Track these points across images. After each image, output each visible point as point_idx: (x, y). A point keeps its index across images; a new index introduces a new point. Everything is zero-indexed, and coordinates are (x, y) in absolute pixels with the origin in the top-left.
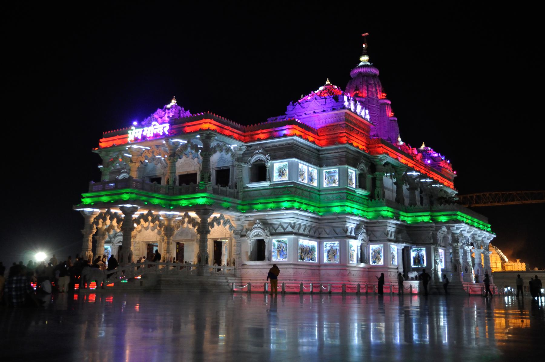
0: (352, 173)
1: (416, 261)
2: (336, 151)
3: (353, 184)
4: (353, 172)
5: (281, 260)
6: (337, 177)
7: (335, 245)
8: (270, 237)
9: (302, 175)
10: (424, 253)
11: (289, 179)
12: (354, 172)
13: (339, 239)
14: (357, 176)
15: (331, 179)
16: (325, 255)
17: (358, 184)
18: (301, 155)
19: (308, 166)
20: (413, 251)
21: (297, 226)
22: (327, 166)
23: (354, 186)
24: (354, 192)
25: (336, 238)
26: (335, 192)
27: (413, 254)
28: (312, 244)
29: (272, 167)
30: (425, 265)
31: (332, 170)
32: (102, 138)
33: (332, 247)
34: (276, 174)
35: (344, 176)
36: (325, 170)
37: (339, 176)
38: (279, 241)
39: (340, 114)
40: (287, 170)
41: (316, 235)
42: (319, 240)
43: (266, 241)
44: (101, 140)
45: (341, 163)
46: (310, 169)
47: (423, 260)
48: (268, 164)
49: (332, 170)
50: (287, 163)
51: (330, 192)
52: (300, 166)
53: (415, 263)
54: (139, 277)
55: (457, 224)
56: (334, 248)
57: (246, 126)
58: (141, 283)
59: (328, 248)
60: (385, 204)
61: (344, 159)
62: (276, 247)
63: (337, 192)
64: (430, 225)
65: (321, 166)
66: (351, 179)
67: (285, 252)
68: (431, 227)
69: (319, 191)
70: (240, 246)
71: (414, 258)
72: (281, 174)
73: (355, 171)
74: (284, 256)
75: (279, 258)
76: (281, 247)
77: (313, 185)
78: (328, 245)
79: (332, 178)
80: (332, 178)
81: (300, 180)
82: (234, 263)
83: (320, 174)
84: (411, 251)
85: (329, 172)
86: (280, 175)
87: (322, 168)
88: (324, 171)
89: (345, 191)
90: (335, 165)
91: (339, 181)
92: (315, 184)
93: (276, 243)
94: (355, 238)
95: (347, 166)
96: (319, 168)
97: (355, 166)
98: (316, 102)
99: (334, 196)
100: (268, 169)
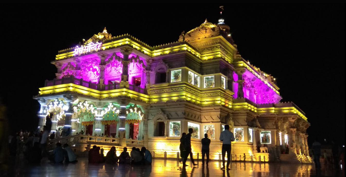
0: (223, 79)
1: (264, 140)
2: (213, 64)
5: (176, 136)
6: (214, 82)
7: (212, 127)
8: (168, 120)
9: (191, 79)
10: (269, 135)
11: (182, 81)
13: (214, 123)
14: (227, 81)
15: (209, 83)
17: (227, 87)
19: (194, 73)
20: (262, 133)
21: (187, 114)
22: (207, 74)
23: (225, 88)
25: (212, 122)
26: (212, 91)
27: (262, 135)
28: (196, 127)
30: (270, 143)
31: (210, 77)
32: (57, 55)
33: (210, 128)
34: (172, 78)
35: (218, 81)
36: (205, 77)
37: (215, 80)
38: (174, 123)
39: (216, 39)
40: (180, 75)
42: (200, 124)
43: (166, 123)
44: (57, 56)
45: (216, 72)
46: (196, 75)
47: (269, 139)
49: (210, 77)
50: (181, 70)
51: (208, 92)
52: (189, 72)
53: (263, 141)
54: (74, 145)
55: (293, 116)
56: (211, 129)
57: (153, 47)
58: (75, 150)
59: (207, 129)
60: (245, 101)
62: (172, 127)
63: (214, 91)
64: (274, 116)
65: (202, 74)
66: (223, 83)
67: (178, 131)
68: (275, 117)
70: (147, 127)
71: (263, 138)
72: (176, 77)
73: (225, 78)
74: (178, 133)
75: (174, 135)
76: (175, 128)
79: (210, 82)
80: (210, 82)
81: (189, 82)
82: (143, 138)
83: (202, 79)
84: (260, 133)
85: (208, 78)
86: (175, 79)
87: (203, 76)
88: (205, 78)
89: (220, 91)
90: (212, 73)
91: (215, 84)
93: (172, 125)
95: (221, 74)
96: (201, 76)
97: (225, 74)
98: (199, 32)
99: (212, 94)
100: (167, 74)
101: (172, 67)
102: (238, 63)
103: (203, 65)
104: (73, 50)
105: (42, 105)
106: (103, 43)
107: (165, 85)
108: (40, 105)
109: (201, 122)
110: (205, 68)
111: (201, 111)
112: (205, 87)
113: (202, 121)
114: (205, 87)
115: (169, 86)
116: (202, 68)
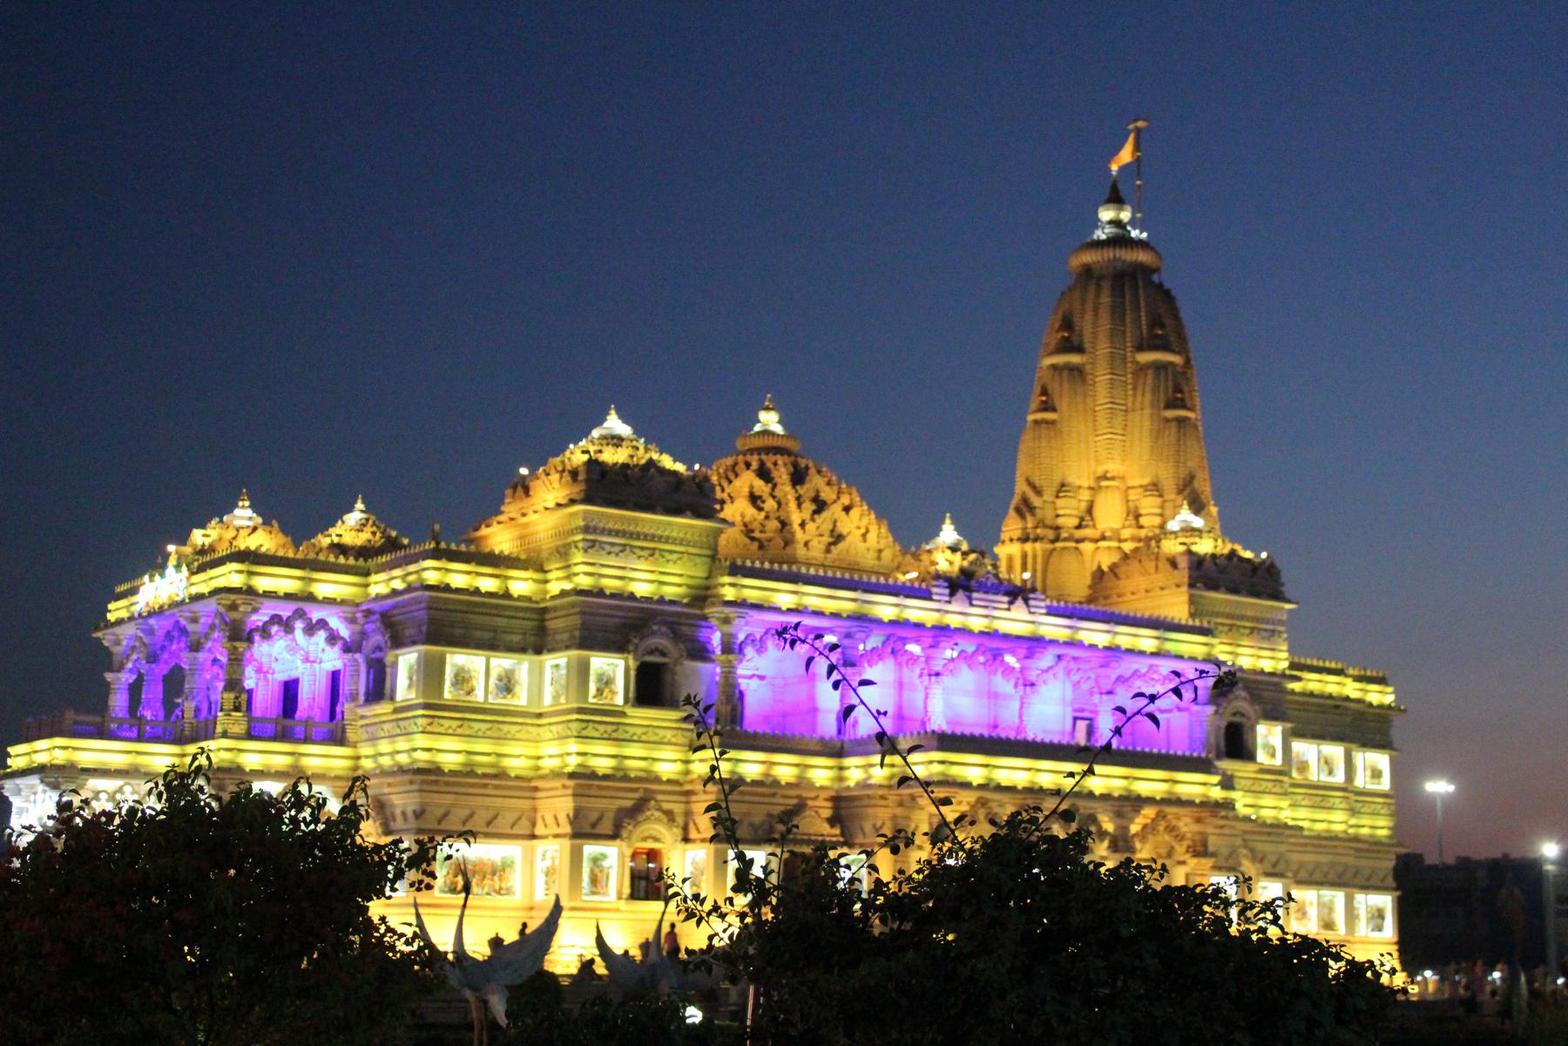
3: (613, 693)
4: (612, 667)
12: (621, 663)
14: (633, 673)
16: (540, 879)
17: (631, 695)
18: (457, 632)
22: (550, 651)
23: (619, 700)
24: (624, 714)
25: (556, 836)
29: (395, 665)
41: (523, 828)
48: (389, 659)
59: (548, 863)
61: (577, 633)
68: (883, 797)
69: (540, 716)
77: (515, 702)
78: (548, 855)
85: (557, 666)
92: (520, 699)
94: (615, 836)
101: (398, 642)
102: (716, 586)
103: (548, 616)
104: (134, 591)
105: (16, 802)
106: (193, 573)
107: (384, 708)
108: (10, 804)
109: (533, 837)
110: (551, 625)
111: (539, 794)
112: (547, 700)
113: (539, 830)
114: (547, 700)
115: (396, 711)
116: (531, 631)
